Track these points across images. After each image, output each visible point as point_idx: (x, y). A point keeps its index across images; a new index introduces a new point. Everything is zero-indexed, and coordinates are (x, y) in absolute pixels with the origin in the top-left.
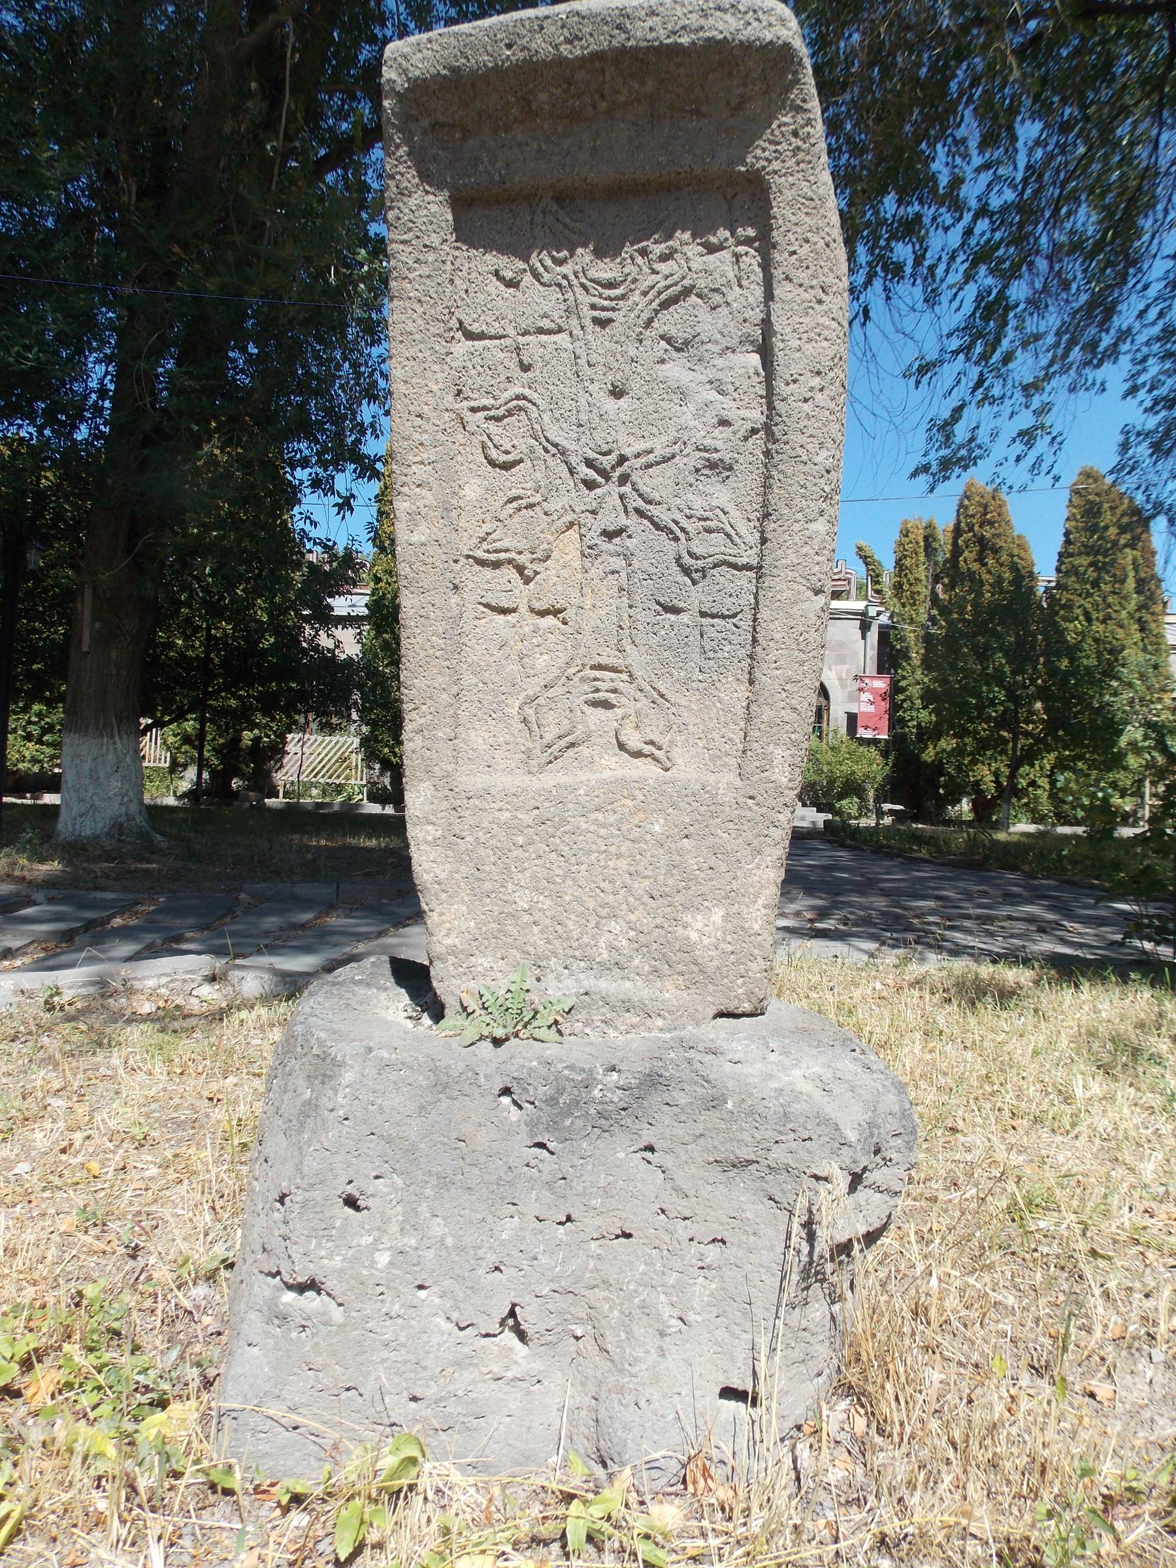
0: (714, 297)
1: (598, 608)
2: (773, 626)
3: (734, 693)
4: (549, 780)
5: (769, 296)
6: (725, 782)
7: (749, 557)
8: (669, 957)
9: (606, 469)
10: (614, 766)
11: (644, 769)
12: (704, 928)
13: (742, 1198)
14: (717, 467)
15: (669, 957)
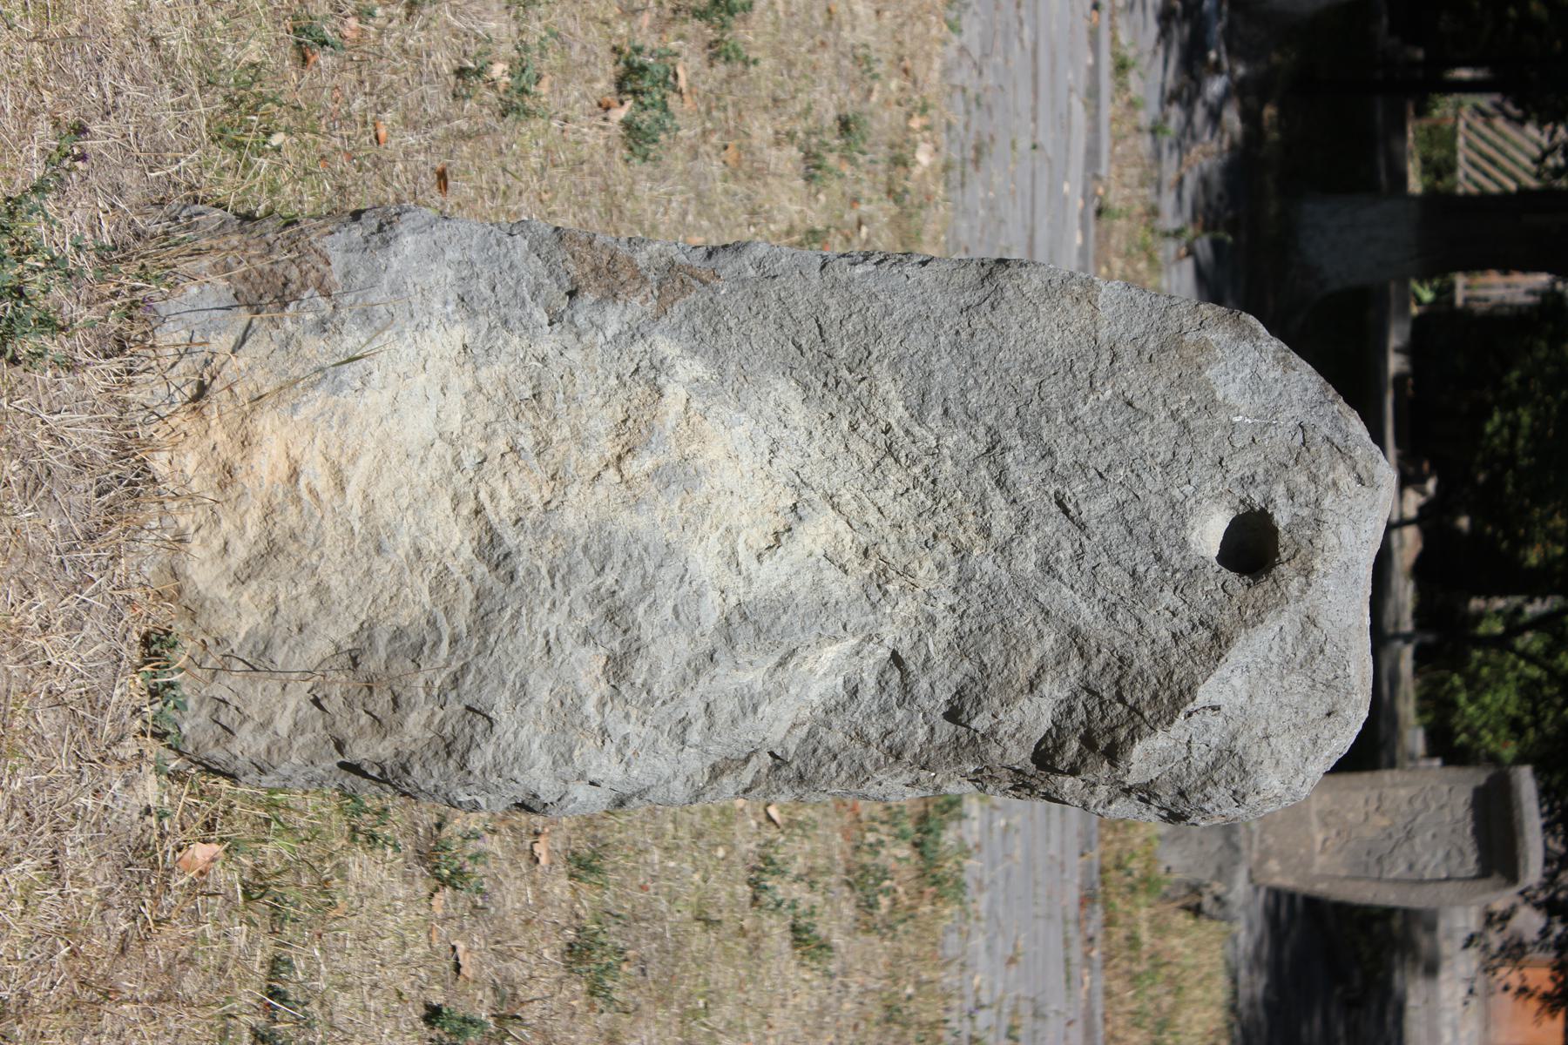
0: (1462, 864)
1: (1368, 833)
2: (1362, 884)
3: (1343, 873)
4: (1315, 820)
5: (1460, 879)
6: (1316, 870)
7: (1385, 876)
8: (1265, 855)
9: (1409, 835)
10: (1319, 837)
11: (1318, 847)
12: (1273, 865)
13: (1212, 871)
14: (1411, 867)
15: (1265, 855)
